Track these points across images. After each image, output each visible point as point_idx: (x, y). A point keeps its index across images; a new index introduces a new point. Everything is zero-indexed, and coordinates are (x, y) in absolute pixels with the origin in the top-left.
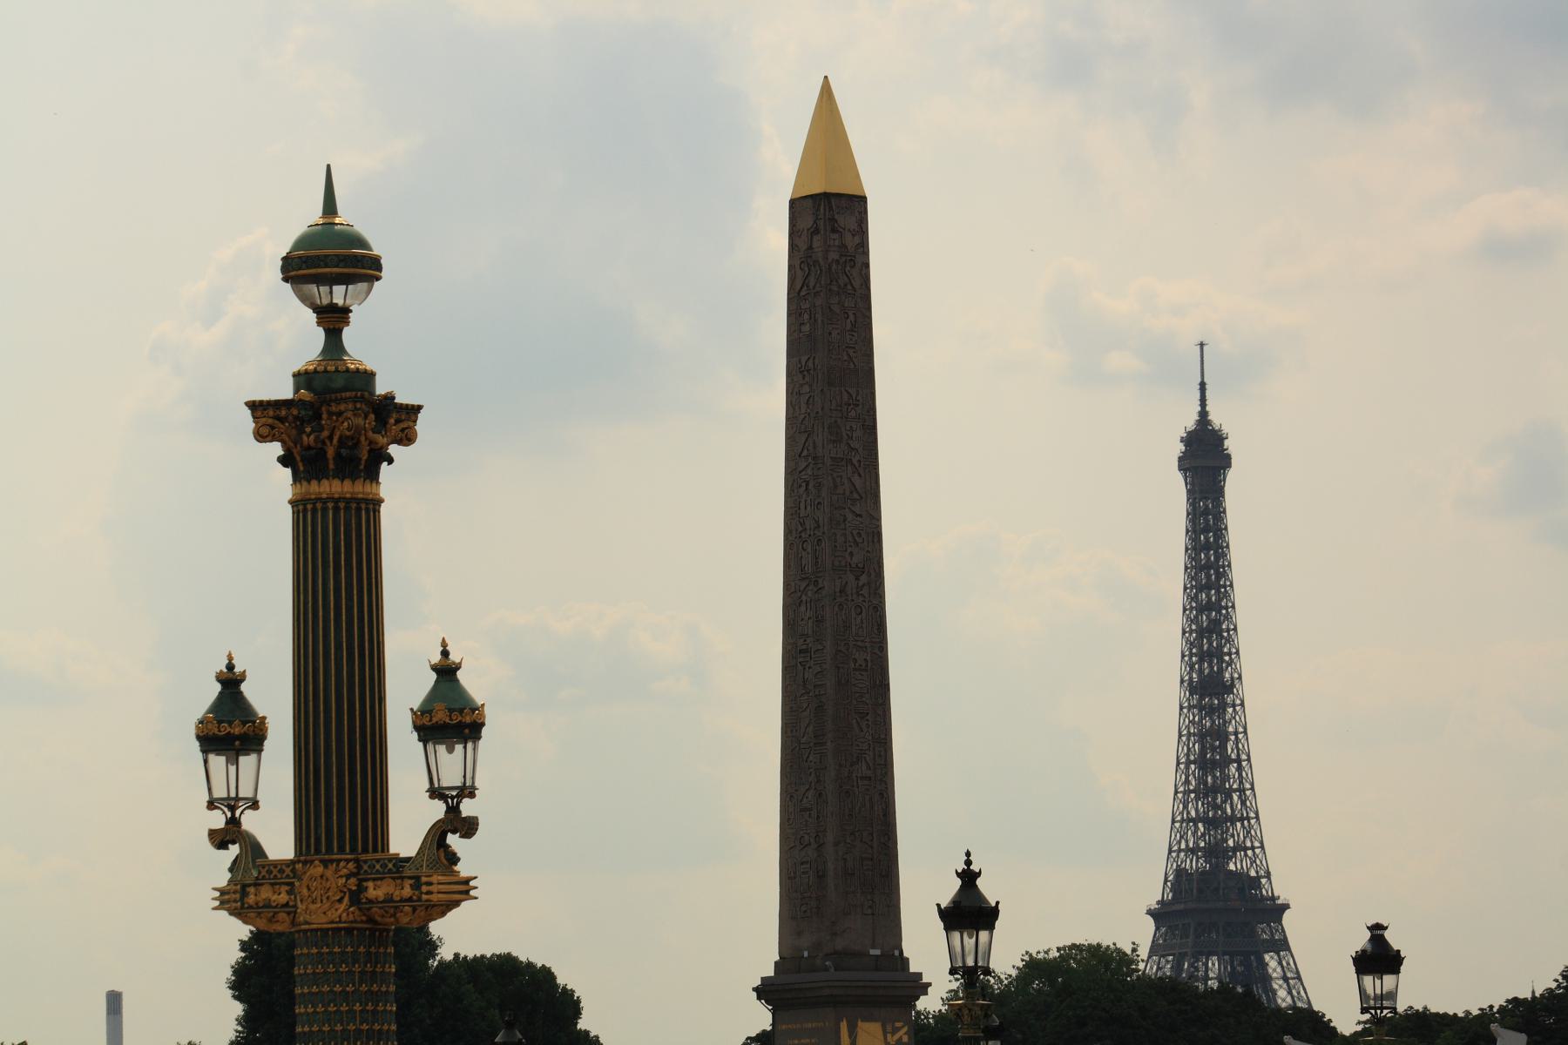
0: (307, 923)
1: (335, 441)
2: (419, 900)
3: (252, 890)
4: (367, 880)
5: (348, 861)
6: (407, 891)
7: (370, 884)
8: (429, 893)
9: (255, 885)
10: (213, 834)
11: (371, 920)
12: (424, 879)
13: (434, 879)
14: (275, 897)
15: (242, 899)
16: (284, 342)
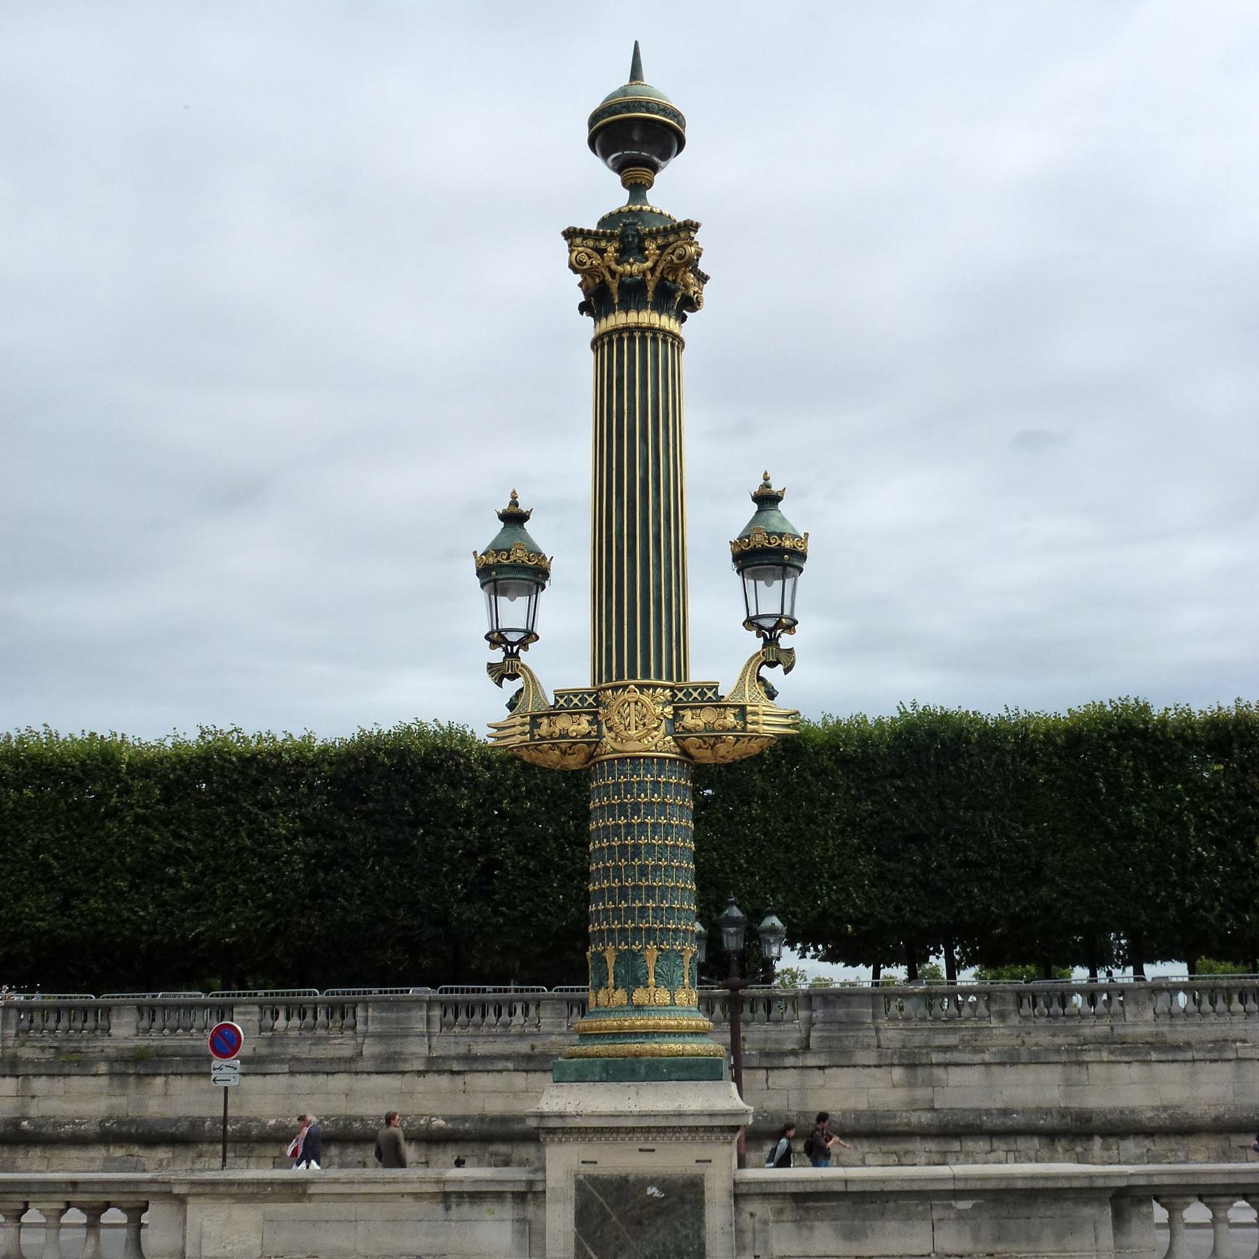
0: (615, 751)
1: (658, 274)
2: (744, 729)
3: (545, 721)
4: (683, 708)
5: (664, 687)
6: (731, 720)
7: (688, 713)
8: (754, 723)
9: (548, 715)
10: (491, 667)
11: (684, 752)
12: (749, 708)
13: (761, 709)
14: (575, 727)
15: (531, 732)
16: (600, 192)
